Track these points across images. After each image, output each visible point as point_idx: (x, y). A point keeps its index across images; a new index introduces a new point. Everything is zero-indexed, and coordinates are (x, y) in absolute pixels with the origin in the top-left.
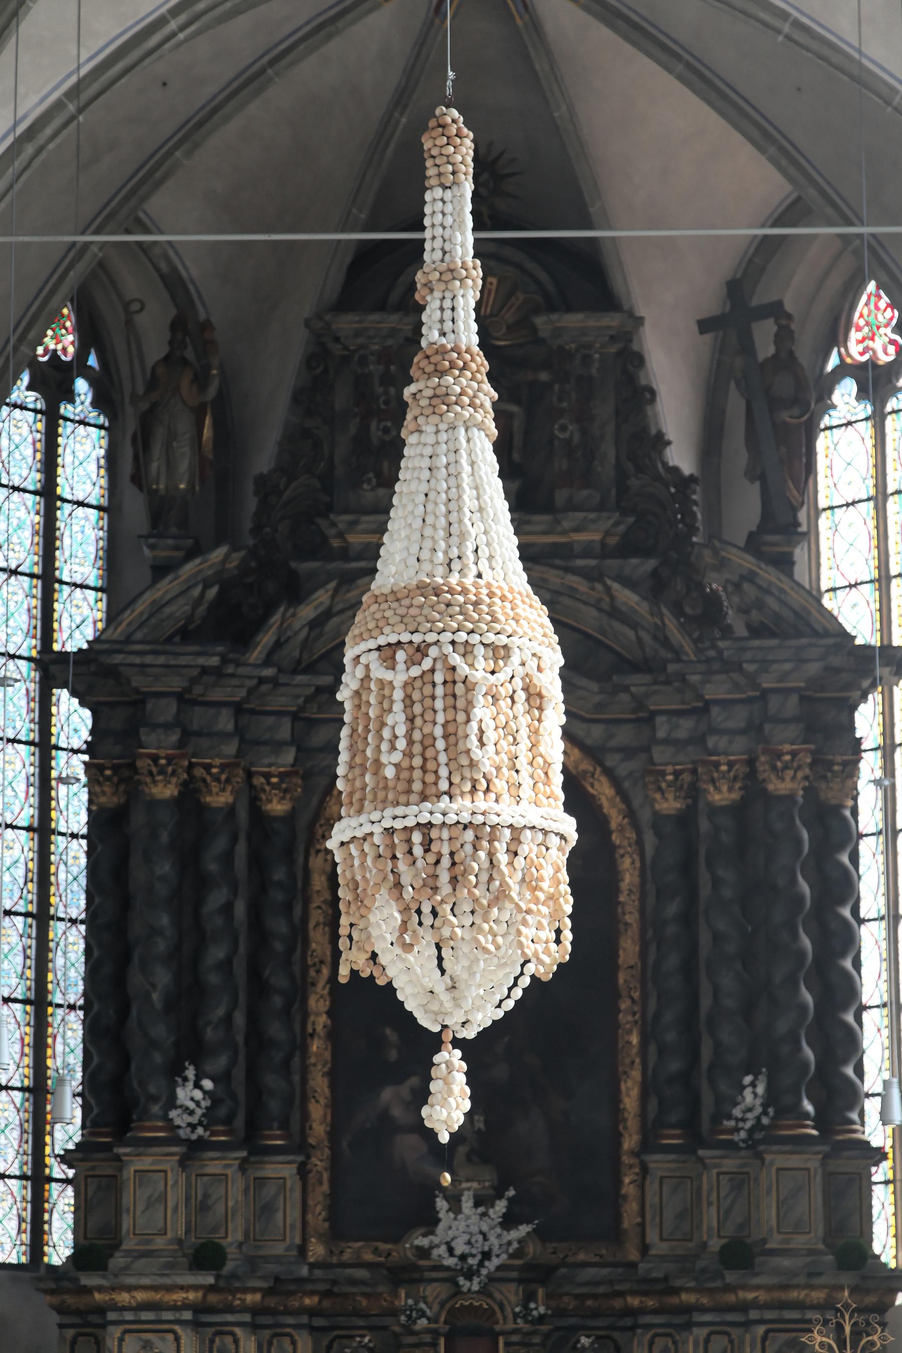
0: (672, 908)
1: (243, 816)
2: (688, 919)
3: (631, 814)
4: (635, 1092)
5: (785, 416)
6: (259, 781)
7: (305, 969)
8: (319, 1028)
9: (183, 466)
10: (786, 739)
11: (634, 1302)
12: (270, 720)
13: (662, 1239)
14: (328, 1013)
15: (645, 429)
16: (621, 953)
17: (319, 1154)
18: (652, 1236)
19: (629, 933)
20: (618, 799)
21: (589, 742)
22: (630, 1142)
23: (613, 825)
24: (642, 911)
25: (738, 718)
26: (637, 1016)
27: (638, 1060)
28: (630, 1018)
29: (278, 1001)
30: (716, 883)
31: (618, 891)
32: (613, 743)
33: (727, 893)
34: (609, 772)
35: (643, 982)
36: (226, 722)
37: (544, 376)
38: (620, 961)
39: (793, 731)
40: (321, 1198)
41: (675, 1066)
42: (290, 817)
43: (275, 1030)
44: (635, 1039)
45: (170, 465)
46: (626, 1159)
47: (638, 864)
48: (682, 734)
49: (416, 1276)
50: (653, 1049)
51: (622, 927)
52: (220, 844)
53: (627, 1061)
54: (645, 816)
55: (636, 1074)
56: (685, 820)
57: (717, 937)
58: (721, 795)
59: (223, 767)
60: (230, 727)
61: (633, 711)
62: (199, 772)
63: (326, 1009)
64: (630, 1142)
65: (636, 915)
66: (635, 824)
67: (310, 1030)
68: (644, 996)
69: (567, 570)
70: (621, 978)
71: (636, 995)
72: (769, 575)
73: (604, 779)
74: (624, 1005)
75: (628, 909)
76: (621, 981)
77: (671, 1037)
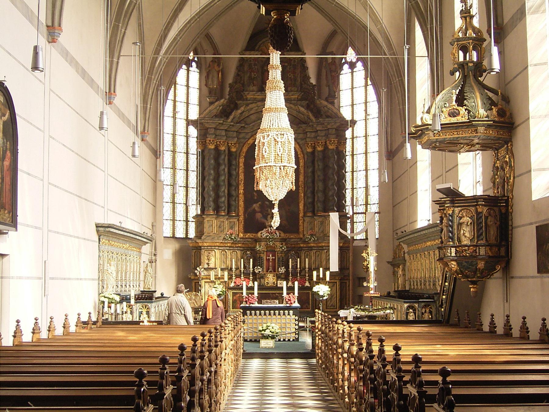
0: (310, 170)
1: (227, 152)
2: (313, 172)
3: (302, 151)
4: (302, 205)
5: (333, 74)
6: (230, 145)
7: (238, 181)
9: (215, 82)
10: (333, 139)
12: (232, 133)
15: (306, 75)
24: (304, 170)
25: (323, 133)
29: (234, 188)
30: (318, 166)
33: (321, 167)
35: (304, 184)
36: (223, 133)
37: (286, 64)
39: (334, 136)
41: (310, 200)
42: (236, 152)
43: (234, 193)
44: (302, 195)
45: (213, 81)
48: (313, 136)
52: (223, 157)
54: (305, 152)
55: (303, 202)
56: (313, 153)
57: (318, 176)
58: (320, 149)
59: (223, 142)
60: (224, 134)
62: (218, 143)
66: (303, 154)
68: (304, 187)
69: (290, 103)
70: (300, 183)
72: (330, 106)
74: (300, 188)
77: (309, 195)
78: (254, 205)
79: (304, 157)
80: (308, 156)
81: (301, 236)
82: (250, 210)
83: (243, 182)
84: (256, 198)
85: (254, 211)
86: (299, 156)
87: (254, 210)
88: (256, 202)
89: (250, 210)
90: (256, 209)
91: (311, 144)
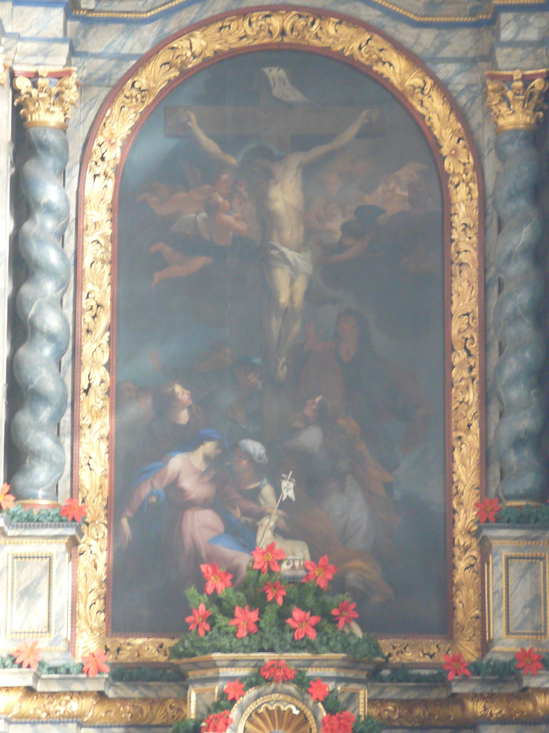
4: (473, 461)
8: (96, 382)
11: (477, 708)
13: (508, 632)
14: (108, 366)
16: (454, 298)
17: (93, 531)
18: (497, 628)
19: (465, 274)
20: (453, 118)
21: (418, 50)
22: (465, 518)
23: (445, 150)
26: (475, 372)
27: (475, 424)
28: (465, 374)
31: (451, 226)
32: (447, 52)
34: (442, 86)
38: (454, 308)
40: (95, 585)
44: (472, 396)
46: (461, 540)
47: (476, 194)
49: (210, 673)
50: (494, 409)
51: (455, 268)
53: (463, 424)
54: (486, 135)
55: (473, 439)
61: (472, 15)
63: (105, 359)
64: (465, 518)
65: (475, 254)
66: (474, 148)
67: (84, 385)
71: (473, 347)
73: (434, 94)
74: (459, 357)
75: (463, 246)
76: (454, 332)
78: (177, 463)
79: (479, 168)
80: (502, 157)
81: (469, 651)
82: (148, 489)
83: (105, 319)
84: (184, 417)
85: (176, 501)
86: (449, 165)
87: (174, 486)
88: (188, 442)
89: (148, 489)
90: (189, 484)
91: (527, 80)
